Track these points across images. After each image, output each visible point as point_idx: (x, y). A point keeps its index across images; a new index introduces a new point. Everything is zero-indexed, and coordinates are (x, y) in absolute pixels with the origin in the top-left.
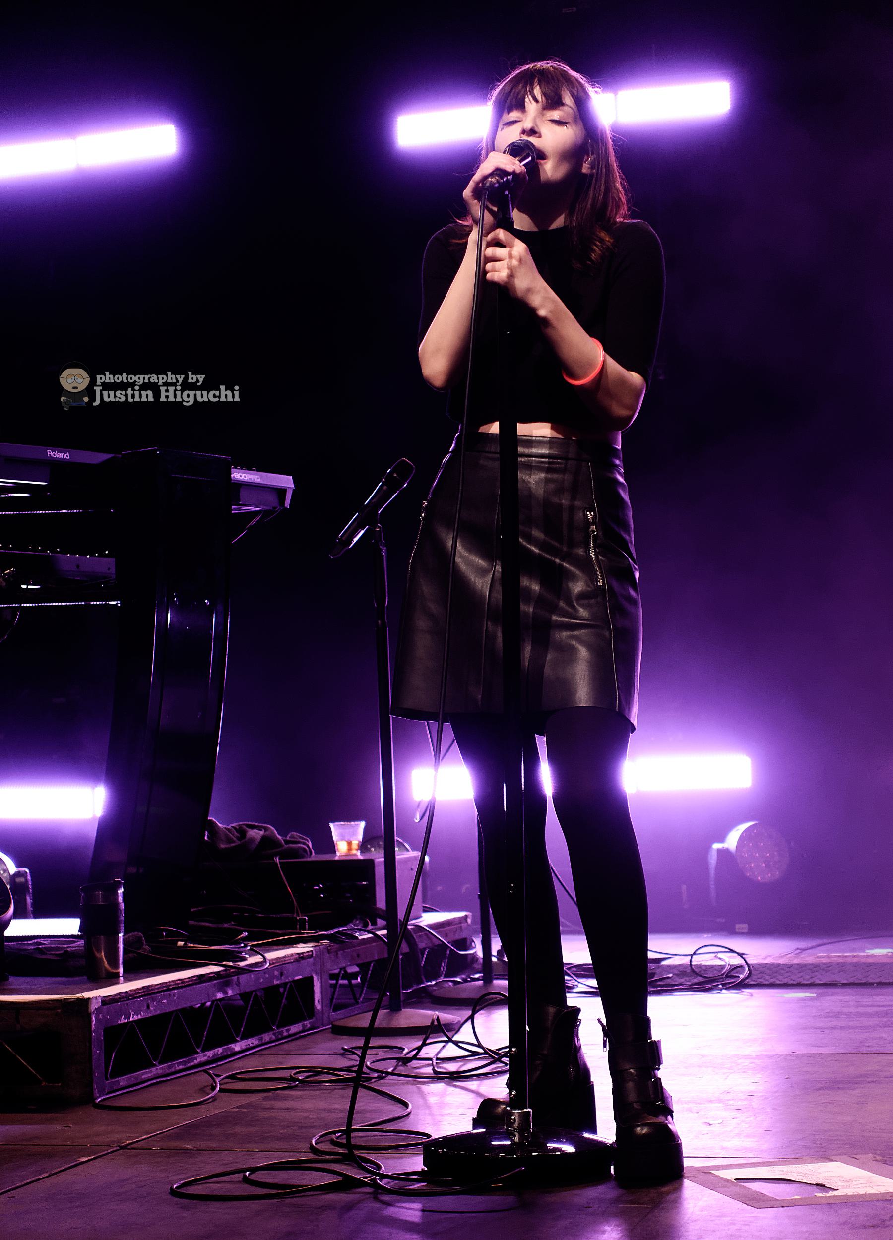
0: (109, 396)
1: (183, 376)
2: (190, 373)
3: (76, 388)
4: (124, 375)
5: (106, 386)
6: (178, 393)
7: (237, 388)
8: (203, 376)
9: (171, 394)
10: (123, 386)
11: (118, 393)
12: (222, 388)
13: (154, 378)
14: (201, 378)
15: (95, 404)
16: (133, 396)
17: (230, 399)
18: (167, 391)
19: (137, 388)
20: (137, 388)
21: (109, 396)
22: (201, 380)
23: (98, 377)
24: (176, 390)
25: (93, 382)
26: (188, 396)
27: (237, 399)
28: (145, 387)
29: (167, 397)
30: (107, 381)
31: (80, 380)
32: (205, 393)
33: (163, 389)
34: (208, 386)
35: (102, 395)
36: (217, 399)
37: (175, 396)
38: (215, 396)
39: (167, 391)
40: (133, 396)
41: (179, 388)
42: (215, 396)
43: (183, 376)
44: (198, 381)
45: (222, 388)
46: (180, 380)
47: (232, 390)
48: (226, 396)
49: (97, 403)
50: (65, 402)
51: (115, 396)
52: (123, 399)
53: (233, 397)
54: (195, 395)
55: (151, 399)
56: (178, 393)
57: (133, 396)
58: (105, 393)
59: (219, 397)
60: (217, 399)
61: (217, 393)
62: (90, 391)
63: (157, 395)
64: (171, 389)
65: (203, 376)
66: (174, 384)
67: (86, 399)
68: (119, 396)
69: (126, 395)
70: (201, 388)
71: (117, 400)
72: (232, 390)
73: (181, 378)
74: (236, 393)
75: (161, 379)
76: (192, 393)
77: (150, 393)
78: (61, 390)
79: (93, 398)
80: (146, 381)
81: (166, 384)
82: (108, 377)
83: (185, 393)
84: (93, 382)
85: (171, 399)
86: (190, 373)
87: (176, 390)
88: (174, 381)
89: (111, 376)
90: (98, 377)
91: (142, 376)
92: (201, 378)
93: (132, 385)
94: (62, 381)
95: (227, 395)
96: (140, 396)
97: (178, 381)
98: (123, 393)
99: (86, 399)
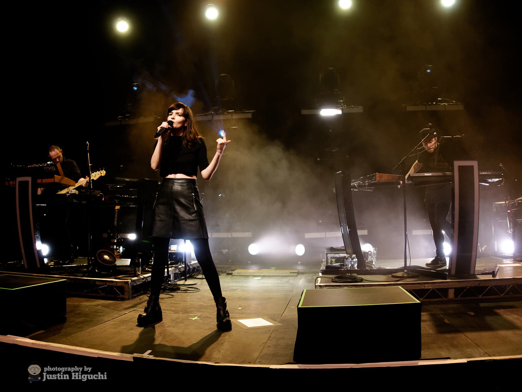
4: (56, 368)
5: (48, 373)
6: (80, 376)
7: (105, 373)
9: (77, 376)
10: (56, 373)
11: (53, 375)
12: (99, 373)
13: (69, 369)
14: (90, 369)
16: (60, 377)
17: (103, 378)
18: (75, 375)
19: (62, 373)
20: (62, 373)
22: (90, 370)
23: (45, 368)
25: (42, 371)
26: (84, 377)
27: (106, 378)
28: (65, 373)
29: (75, 377)
31: (37, 370)
32: (92, 375)
33: (73, 374)
34: (93, 372)
35: (46, 377)
37: (78, 377)
38: (96, 377)
39: (75, 375)
41: (80, 373)
44: (88, 370)
45: (99, 373)
46: (81, 370)
47: (104, 374)
49: (44, 380)
50: (30, 380)
52: (56, 378)
53: (104, 377)
55: (68, 378)
56: (80, 376)
57: (60, 377)
58: (48, 375)
61: (97, 376)
62: (41, 375)
63: (71, 376)
64: (77, 374)
66: (78, 372)
67: (39, 378)
68: (54, 377)
69: (57, 377)
70: (90, 373)
72: (104, 374)
73: (81, 369)
74: (105, 376)
75: (72, 369)
76: (86, 376)
77: (67, 375)
79: (42, 378)
81: (75, 372)
82: (49, 369)
84: (42, 371)
85: (77, 378)
90: (45, 368)
92: (90, 369)
93: (60, 372)
94: (29, 370)
96: (63, 377)
99: (39, 378)
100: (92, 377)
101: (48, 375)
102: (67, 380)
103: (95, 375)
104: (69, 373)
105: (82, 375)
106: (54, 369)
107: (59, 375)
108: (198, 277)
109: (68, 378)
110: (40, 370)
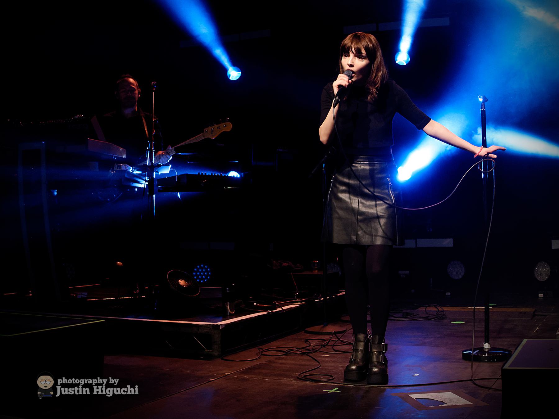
0: (65, 391)
1: (106, 380)
2: (110, 378)
3: (46, 387)
4: (73, 380)
5: (63, 386)
6: (104, 390)
7: (137, 386)
8: (118, 380)
9: (100, 390)
10: (73, 386)
11: (70, 389)
12: (129, 386)
13: (90, 381)
14: (117, 381)
15: (57, 396)
16: (78, 391)
17: (133, 393)
18: (97, 388)
20: (80, 386)
21: (65, 391)
22: (117, 382)
23: (59, 380)
25: (56, 383)
26: (109, 391)
27: (137, 393)
28: (85, 386)
29: (98, 392)
30: (64, 383)
31: (48, 382)
32: (119, 389)
33: (95, 387)
34: (120, 386)
35: (61, 391)
36: (126, 393)
37: (102, 391)
39: (97, 388)
40: (78, 391)
41: (104, 387)
42: (124, 391)
43: (106, 380)
44: (115, 383)
45: (129, 386)
48: (131, 391)
50: (40, 395)
51: (68, 391)
52: (73, 393)
54: (113, 391)
55: (88, 393)
56: (104, 390)
57: (78, 391)
58: (63, 389)
59: (127, 392)
60: (126, 393)
61: (126, 390)
62: (54, 388)
63: (92, 391)
64: (100, 387)
65: (118, 380)
66: (101, 385)
67: (52, 393)
68: (71, 391)
69: (74, 391)
70: (117, 387)
71: (69, 393)
73: (105, 381)
74: (137, 390)
75: (94, 382)
76: (111, 389)
77: (88, 389)
78: (37, 388)
79: (56, 393)
80: (86, 382)
82: (64, 381)
83: (108, 389)
84: (56, 383)
85: (100, 393)
86: (110, 378)
88: (101, 382)
89: (66, 380)
90: (59, 380)
91: (83, 380)
92: (117, 381)
93: (78, 385)
94: (38, 383)
95: (132, 391)
96: (82, 392)
97: (103, 383)
98: (73, 389)
99: (52, 393)
100: (120, 391)
101: (63, 389)
102: (87, 395)
103: (123, 389)
104: (91, 387)
105: (106, 388)
106: (70, 381)
107: (76, 389)
109: (88, 393)
110: (53, 383)
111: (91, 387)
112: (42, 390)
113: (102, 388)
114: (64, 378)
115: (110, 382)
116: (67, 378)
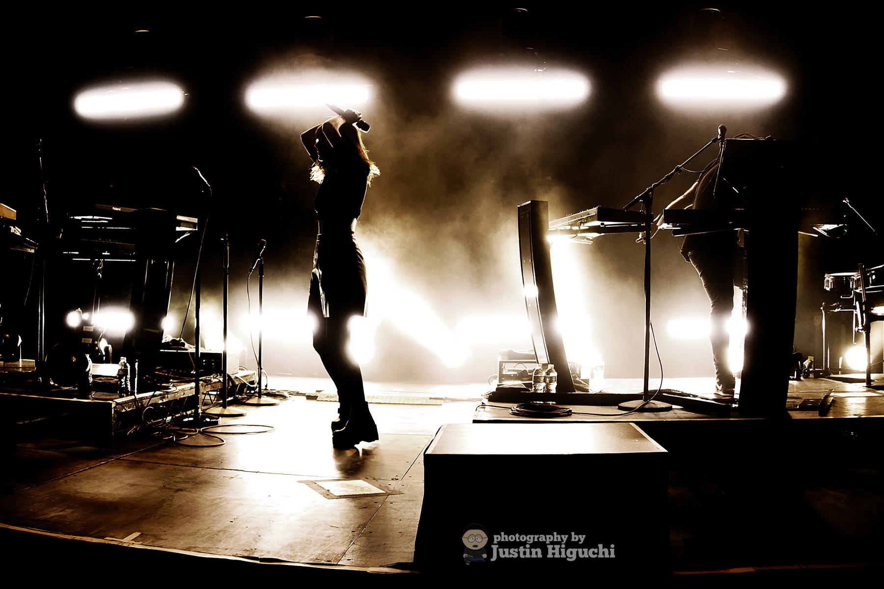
0: (504, 553)
2: (573, 533)
3: (476, 546)
4: (517, 535)
5: (502, 545)
6: (563, 551)
7: (612, 546)
9: (557, 551)
10: (516, 545)
11: (512, 550)
12: (600, 546)
13: (542, 538)
14: (582, 538)
15: (492, 560)
16: (525, 553)
17: (607, 556)
18: (554, 549)
19: (528, 546)
20: (528, 546)
21: (504, 553)
23: (495, 536)
24: (560, 548)
25: (491, 541)
26: (571, 553)
27: (613, 556)
28: (535, 545)
29: (554, 554)
31: (479, 540)
32: (586, 550)
33: (550, 547)
34: (588, 545)
35: (498, 552)
37: (560, 553)
38: (594, 553)
39: (554, 549)
40: (524, 553)
41: (563, 546)
42: (594, 553)
44: (579, 540)
45: (600, 546)
46: (565, 540)
47: (609, 548)
48: (604, 553)
49: (494, 559)
50: (467, 559)
52: (516, 556)
53: (610, 553)
54: (577, 552)
55: (540, 556)
56: (563, 551)
57: (525, 553)
58: (501, 550)
59: (598, 554)
61: (596, 551)
62: (488, 549)
64: (557, 547)
66: (559, 543)
67: (485, 556)
68: (513, 553)
69: (519, 553)
70: (582, 546)
71: (511, 556)
72: (609, 548)
74: (612, 551)
75: (548, 539)
76: (574, 550)
77: (539, 550)
79: (490, 555)
80: (536, 540)
81: (553, 543)
82: (503, 537)
83: (569, 550)
84: (491, 541)
85: (557, 556)
86: (573, 533)
87: (560, 548)
90: (495, 536)
91: (532, 536)
92: (582, 538)
93: (524, 544)
94: (464, 540)
95: (604, 552)
96: (531, 553)
98: (516, 550)
99: (485, 556)
100: (587, 553)
102: (537, 558)
104: (543, 546)
105: (566, 549)
106: (512, 538)
107: (522, 549)
108: (250, 401)
109: (540, 556)
110: (486, 540)
111: (543, 546)
112: (470, 551)
113: (561, 548)
114: (502, 533)
115: (573, 540)
116: (508, 533)
